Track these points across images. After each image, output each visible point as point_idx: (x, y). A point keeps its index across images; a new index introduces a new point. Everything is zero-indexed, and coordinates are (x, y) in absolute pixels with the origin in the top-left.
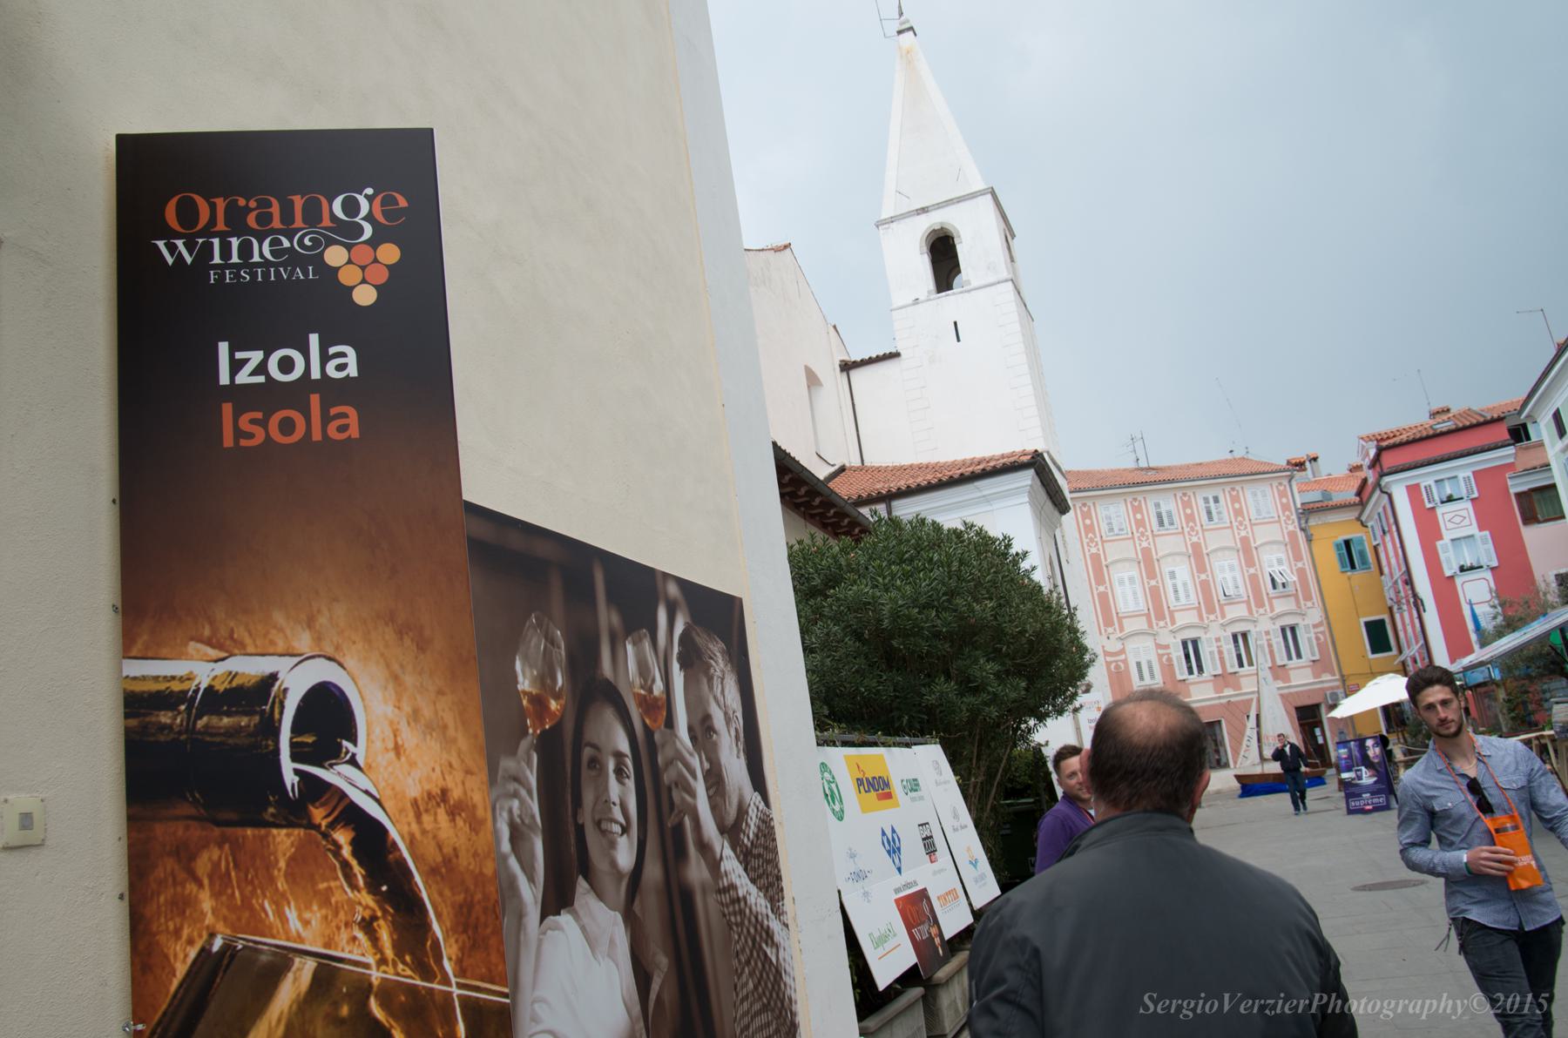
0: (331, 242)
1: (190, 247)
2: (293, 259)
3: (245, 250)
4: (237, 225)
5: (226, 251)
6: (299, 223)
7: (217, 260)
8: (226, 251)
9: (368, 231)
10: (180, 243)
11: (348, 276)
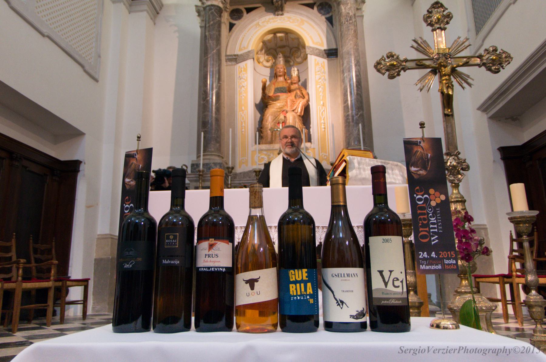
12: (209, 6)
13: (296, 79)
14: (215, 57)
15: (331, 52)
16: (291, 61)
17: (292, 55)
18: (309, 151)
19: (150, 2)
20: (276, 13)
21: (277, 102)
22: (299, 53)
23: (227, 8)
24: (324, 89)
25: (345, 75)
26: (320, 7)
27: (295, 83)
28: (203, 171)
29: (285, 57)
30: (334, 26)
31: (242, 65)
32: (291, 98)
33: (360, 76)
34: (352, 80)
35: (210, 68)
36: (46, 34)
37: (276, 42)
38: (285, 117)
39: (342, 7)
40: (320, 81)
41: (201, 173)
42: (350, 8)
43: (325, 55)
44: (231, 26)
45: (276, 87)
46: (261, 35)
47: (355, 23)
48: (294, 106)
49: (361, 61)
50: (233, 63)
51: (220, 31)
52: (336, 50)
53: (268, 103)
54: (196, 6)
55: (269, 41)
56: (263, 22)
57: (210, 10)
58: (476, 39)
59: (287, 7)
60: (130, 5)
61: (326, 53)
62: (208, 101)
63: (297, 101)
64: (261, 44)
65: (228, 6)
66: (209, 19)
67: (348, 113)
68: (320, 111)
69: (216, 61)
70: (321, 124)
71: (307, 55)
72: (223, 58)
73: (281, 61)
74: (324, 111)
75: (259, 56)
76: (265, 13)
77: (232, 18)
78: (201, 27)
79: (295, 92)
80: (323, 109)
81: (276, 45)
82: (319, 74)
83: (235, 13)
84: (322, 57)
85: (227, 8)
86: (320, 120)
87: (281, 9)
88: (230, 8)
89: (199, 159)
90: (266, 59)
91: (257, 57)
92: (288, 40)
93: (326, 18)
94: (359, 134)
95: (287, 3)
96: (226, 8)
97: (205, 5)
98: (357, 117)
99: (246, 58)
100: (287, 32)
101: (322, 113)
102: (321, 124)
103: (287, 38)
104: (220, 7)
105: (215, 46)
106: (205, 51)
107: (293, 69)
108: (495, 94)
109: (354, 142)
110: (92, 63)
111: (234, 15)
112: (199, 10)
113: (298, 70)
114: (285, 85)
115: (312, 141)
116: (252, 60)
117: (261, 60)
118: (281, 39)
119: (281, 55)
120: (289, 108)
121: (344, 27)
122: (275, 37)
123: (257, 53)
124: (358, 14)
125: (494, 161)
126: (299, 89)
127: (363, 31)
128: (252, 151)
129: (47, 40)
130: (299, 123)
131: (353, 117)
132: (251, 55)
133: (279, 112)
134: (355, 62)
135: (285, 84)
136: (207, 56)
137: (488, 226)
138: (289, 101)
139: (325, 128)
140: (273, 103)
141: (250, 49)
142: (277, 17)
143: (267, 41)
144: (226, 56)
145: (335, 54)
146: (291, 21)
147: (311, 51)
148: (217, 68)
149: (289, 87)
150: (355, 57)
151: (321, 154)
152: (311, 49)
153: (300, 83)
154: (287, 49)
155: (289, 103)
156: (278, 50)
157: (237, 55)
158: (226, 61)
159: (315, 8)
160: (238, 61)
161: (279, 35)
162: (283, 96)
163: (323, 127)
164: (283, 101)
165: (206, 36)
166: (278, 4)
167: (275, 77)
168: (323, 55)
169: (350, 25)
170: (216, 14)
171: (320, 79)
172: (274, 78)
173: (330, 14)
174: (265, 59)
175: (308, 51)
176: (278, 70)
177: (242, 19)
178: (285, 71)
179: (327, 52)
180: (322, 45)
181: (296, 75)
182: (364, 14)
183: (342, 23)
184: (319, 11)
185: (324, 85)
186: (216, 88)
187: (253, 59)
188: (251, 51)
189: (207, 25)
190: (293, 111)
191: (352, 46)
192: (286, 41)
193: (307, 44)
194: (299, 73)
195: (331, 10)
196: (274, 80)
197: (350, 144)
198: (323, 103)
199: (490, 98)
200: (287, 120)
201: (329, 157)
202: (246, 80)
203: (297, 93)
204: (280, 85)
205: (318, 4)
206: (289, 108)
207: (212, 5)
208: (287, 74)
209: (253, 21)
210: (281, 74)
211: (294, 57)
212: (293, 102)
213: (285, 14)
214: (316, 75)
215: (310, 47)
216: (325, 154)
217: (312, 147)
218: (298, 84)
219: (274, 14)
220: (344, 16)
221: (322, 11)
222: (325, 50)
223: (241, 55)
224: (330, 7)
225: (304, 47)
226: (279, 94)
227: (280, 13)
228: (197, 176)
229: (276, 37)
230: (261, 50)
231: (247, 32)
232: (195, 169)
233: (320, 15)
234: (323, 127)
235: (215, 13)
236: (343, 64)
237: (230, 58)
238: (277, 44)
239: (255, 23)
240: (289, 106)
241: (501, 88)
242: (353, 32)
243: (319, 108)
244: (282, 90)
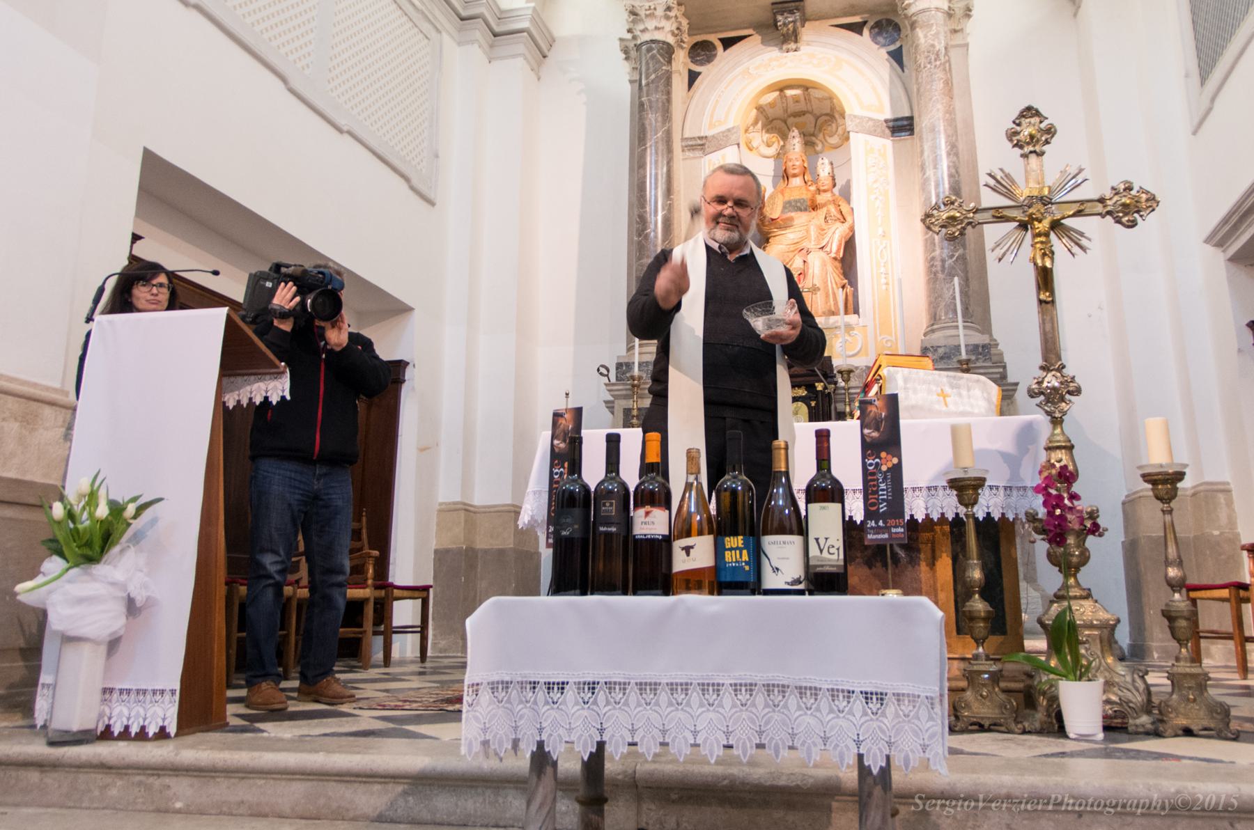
0: (880, 469)
1: (881, 503)
2: (885, 479)
3: (883, 490)
4: (876, 492)
5: (883, 495)
6: (875, 477)
7: (885, 497)
8: (883, 495)
9: (877, 460)
10: (881, 506)
11: (890, 465)
12: (647, 42)
13: (827, 182)
14: (661, 147)
15: (900, 123)
16: (818, 142)
17: (820, 130)
18: (855, 332)
19: (529, 39)
20: (785, 47)
21: (787, 231)
22: (834, 125)
23: (684, 42)
25: (927, 174)
26: (876, 30)
27: (825, 191)
28: (640, 378)
29: (804, 135)
30: (905, 70)
32: (818, 223)
33: (959, 176)
34: (941, 186)
35: (651, 168)
36: (345, 128)
37: (785, 105)
38: (804, 262)
39: (920, 33)
40: (875, 186)
41: (636, 382)
42: (937, 33)
43: (888, 132)
44: (693, 77)
45: (787, 199)
46: (753, 95)
47: (947, 65)
48: (823, 239)
49: (961, 146)
50: (698, 153)
51: (669, 93)
52: (911, 119)
53: (770, 233)
54: (621, 40)
55: (772, 105)
57: (649, 50)
58: (1200, 94)
59: (807, 33)
60: (491, 46)
61: (889, 127)
62: (647, 237)
63: (829, 228)
64: (755, 111)
65: (686, 37)
66: (648, 69)
67: (933, 254)
69: (663, 154)
71: (849, 132)
72: (677, 145)
73: (796, 143)
74: (885, 247)
75: (750, 136)
76: (763, 47)
78: (631, 82)
79: (825, 210)
80: (884, 245)
81: (786, 111)
82: (874, 172)
83: (699, 51)
85: (684, 42)
87: (793, 38)
88: (689, 41)
89: (631, 352)
90: (765, 140)
91: (747, 138)
92: (810, 101)
93: (889, 53)
94: (954, 298)
95: (807, 24)
96: (682, 41)
97: (639, 42)
98: (950, 261)
99: (723, 143)
100: (806, 86)
101: (882, 251)
103: (808, 99)
104: (668, 44)
105: (659, 124)
106: (640, 136)
107: (820, 161)
108: (1234, 213)
109: (946, 314)
110: (424, 170)
111: (698, 55)
112: (627, 47)
113: (832, 164)
114: (806, 195)
115: (861, 310)
116: (736, 146)
117: (755, 144)
118: (796, 100)
119: (795, 132)
120: (813, 243)
121: (924, 74)
122: (782, 96)
123: (746, 131)
124: (958, 39)
125: (1240, 351)
126: (834, 202)
127: (967, 79)
129: (347, 137)
130: (835, 275)
131: (943, 261)
132: (733, 137)
133: (793, 251)
134: (946, 147)
135: (804, 192)
136: (645, 144)
137: (1232, 486)
138: (812, 227)
139: (887, 284)
140: (779, 233)
141: (730, 125)
142: (785, 54)
143: (766, 105)
144: (683, 139)
145: (908, 127)
148: (665, 169)
149: (813, 201)
150: (948, 136)
152: (858, 121)
153: (836, 190)
154: (809, 119)
155: (812, 233)
156: (791, 120)
157: (706, 137)
158: (683, 151)
159: (866, 31)
160: (708, 150)
161: (789, 93)
162: (800, 218)
163: (883, 281)
164: (800, 229)
165: (642, 105)
166: (788, 29)
167: (783, 177)
168: (883, 132)
169: (936, 70)
170: (662, 60)
171: (875, 182)
172: (782, 181)
173: (898, 44)
174: (763, 142)
175: (850, 125)
176: (790, 164)
178: (806, 165)
179: (891, 124)
181: (827, 174)
182: (969, 40)
183: (920, 66)
184: (874, 39)
186: (663, 209)
187: (738, 144)
188: (733, 128)
189: (644, 82)
190: (822, 248)
191: (941, 115)
192: (807, 103)
193: (848, 112)
194: (833, 168)
195: (899, 35)
196: (782, 184)
197: (938, 317)
198: (884, 232)
199: (1225, 221)
200: (808, 268)
201: (897, 344)
203: (828, 212)
204: (795, 195)
205: (871, 23)
206: (813, 243)
207: (653, 41)
208: (808, 172)
210: (796, 171)
211: (824, 135)
212: (821, 230)
213: (802, 48)
215: (855, 116)
217: (861, 324)
218: (832, 192)
219: (781, 49)
220: (924, 52)
221: (880, 39)
222: (886, 121)
223: (713, 136)
224: (897, 28)
225: (843, 115)
226: (793, 214)
227: (793, 46)
228: (629, 387)
229: (785, 96)
230: (755, 123)
231: (726, 88)
232: (624, 373)
233: (877, 46)
234: (883, 281)
235: (658, 56)
236: (922, 152)
237: (691, 143)
238: (787, 110)
239: (739, 69)
240: (813, 239)
241: (1243, 202)
242: (942, 85)
244: (799, 204)
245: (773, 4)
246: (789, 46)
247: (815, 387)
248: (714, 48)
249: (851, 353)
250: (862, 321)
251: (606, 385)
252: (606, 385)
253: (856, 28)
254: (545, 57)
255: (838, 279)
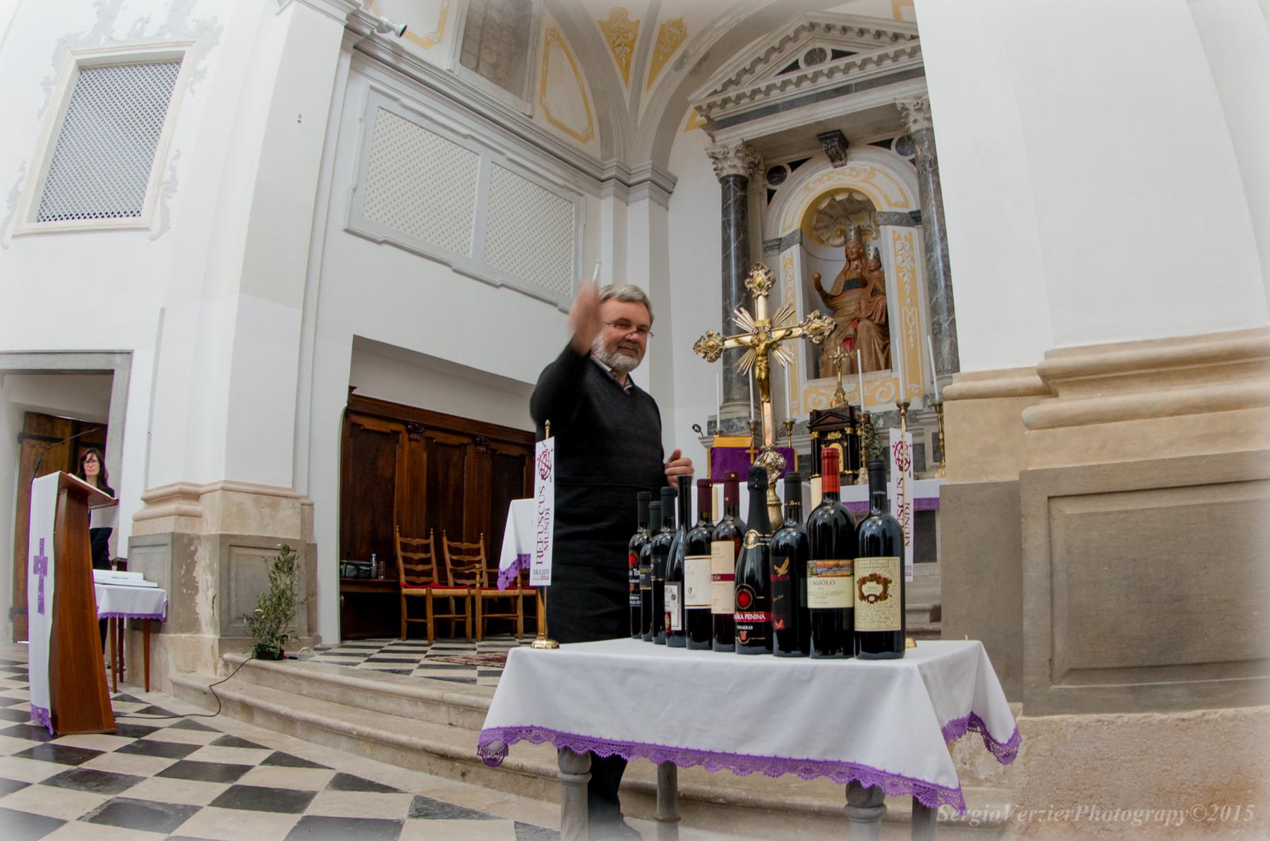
24: (913, 278)
31: (787, 253)
40: (903, 265)
43: (912, 221)
44: (771, 194)
56: (813, 183)
68: (906, 315)
70: (908, 336)
77: (771, 182)
84: (907, 226)
86: (907, 327)
100: (850, 191)
102: (908, 336)
104: (741, 176)
111: (774, 177)
128: (805, 391)
144: (764, 242)
146: (855, 174)
147: (885, 220)
151: (909, 387)
157: (781, 239)
163: (911, 340)
171: (903, 261)
175: (880, 220)
177: (786, 181)
180: (906, 205)
185: (913, 271)
193: (878, 210)
202: (793, 278)
209: (800, 183)
214: (896, 256)
215: (884, 213)
216: (917, 386)
217: (893, 377)
222: (910, 213)
223: (785, 238)
239: (802, 186)
243: (905, 310)
245: (818, 135)
246: (837, 164)
247: (845, 431)
248: (785, 171)
249: (887, 400)
250: (894, 375)
251: (700, 438)
252: (700, 438)
253: (886, 144)
254: (670, 193)
255: (880, 341)
